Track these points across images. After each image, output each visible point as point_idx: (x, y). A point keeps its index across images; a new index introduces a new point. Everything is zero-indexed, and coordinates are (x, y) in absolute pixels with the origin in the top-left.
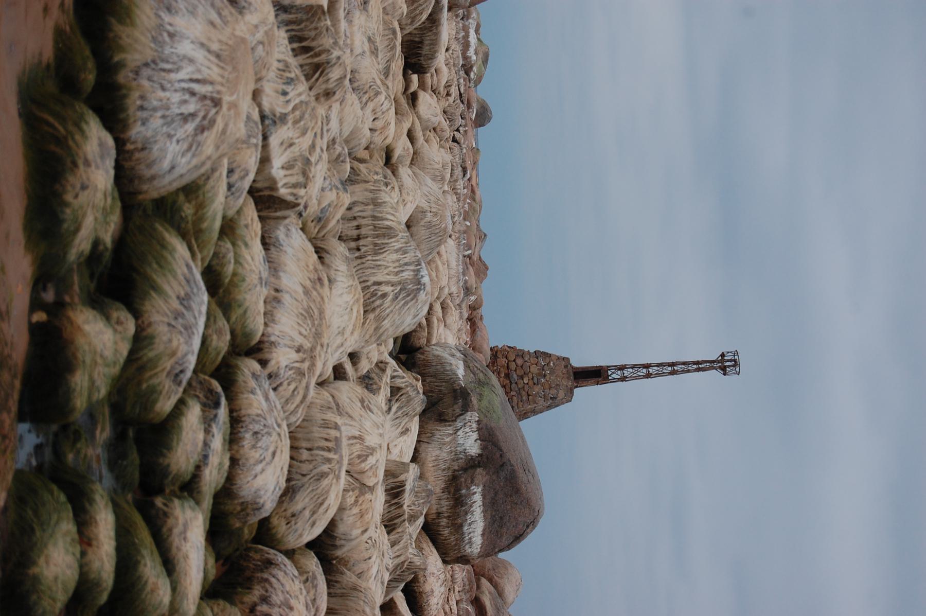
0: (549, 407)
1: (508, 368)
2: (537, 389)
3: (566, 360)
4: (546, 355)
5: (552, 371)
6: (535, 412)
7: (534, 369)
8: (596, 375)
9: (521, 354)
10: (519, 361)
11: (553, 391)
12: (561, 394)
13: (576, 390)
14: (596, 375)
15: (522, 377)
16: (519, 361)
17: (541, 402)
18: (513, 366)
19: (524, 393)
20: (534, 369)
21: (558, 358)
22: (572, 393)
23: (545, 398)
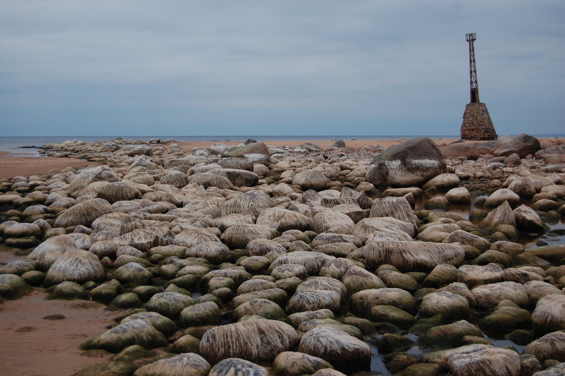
0: (487, 113)
1: (469, 130)
2: (479, 118)
3: (467, 106)
4: (465, 114)
5: (472, 111)
6: (489, 119)
7: (471, 119)
8: (474, 93)
9: (464, 124)
10: (467, 125)
11: (480, 111)
12: (481, 108)
13: (480, 102)
14: (474, 93)
15: (474, 124)
16: (467, 125)
17: (485, 116)
18: (469, 128)
19: (480, 123)
20: (471, 119)
21: (466, 109)
22: (481, 103)
23: (483, 115)
